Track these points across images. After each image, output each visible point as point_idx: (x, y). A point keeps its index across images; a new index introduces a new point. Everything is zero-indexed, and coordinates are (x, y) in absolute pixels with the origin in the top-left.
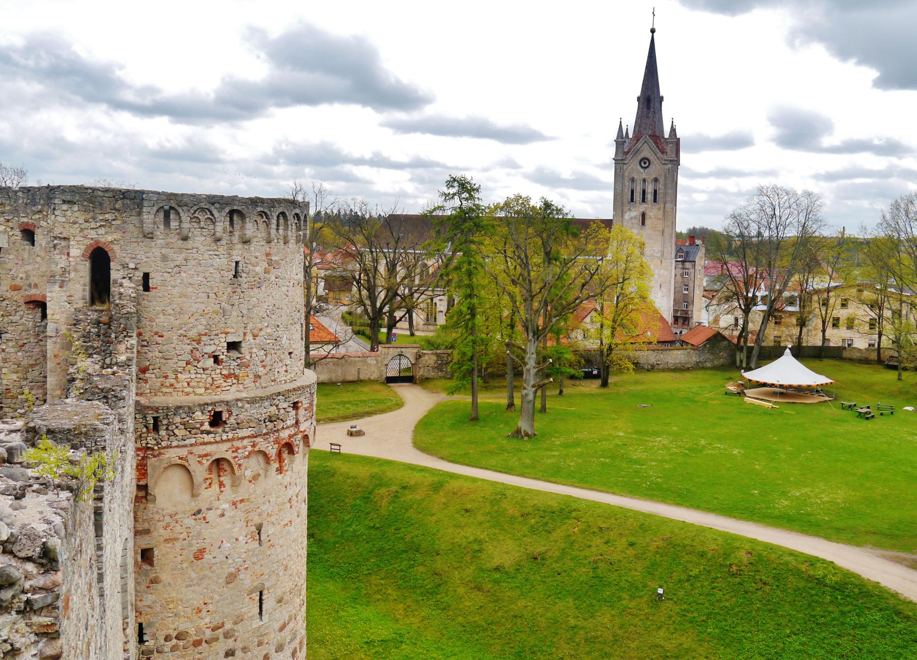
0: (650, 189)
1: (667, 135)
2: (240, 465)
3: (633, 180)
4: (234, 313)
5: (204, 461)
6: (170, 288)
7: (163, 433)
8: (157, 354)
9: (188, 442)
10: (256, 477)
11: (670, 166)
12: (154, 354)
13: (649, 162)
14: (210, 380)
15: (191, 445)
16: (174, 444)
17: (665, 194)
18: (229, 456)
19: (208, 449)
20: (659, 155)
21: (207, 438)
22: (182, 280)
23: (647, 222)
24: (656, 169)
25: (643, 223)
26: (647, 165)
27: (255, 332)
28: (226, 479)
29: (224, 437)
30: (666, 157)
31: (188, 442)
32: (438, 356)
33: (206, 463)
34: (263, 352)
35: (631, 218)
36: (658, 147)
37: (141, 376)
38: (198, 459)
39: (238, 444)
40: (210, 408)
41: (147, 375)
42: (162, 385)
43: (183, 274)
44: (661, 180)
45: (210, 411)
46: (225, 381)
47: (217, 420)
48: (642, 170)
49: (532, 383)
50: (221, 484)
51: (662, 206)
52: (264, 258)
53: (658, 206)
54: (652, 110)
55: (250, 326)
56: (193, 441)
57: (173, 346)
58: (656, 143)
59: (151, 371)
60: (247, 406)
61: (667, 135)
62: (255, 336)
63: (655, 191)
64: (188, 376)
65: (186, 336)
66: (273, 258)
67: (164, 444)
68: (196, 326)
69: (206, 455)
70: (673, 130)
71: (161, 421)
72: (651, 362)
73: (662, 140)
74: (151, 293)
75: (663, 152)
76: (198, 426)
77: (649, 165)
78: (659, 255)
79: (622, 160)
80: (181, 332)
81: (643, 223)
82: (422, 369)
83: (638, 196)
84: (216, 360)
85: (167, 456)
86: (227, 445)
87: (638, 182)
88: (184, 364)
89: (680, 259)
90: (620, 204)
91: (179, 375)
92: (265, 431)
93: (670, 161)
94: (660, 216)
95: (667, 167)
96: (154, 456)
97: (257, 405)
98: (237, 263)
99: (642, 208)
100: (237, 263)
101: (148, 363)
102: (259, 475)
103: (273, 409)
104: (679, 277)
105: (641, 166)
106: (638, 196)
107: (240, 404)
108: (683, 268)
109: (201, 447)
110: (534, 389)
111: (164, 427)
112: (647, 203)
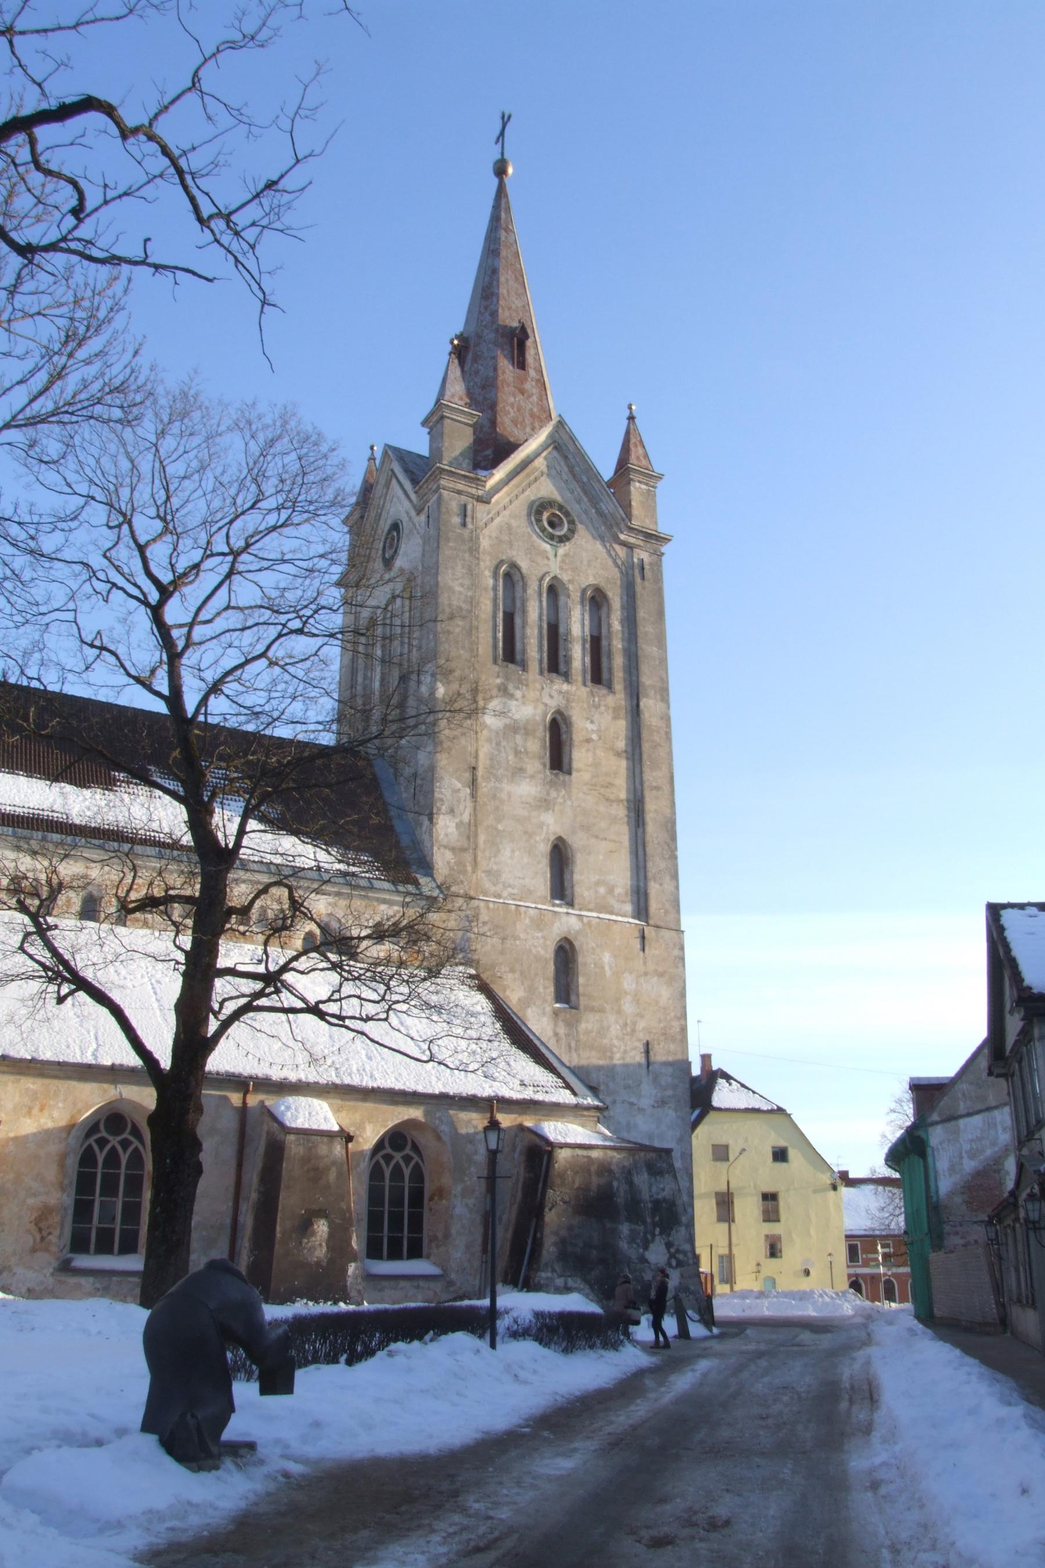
23: (580, 757)
54: (532, 373)
105: (543, 530)
112: (567, 677)
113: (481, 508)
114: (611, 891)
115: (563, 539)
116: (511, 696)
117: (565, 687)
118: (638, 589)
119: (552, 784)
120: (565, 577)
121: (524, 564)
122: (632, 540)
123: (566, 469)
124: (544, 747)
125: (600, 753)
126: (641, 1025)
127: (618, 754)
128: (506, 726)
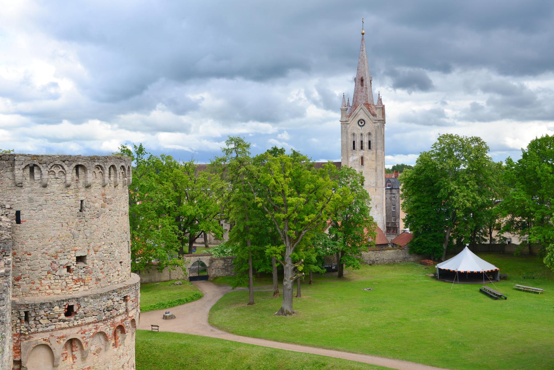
0: (366, 141)
1: (376, 103)
2: (87, 343)
3: (354, 134)
4: (81, 236)
5: (62, 341)
6: (35, 220)
7: (32, 322)
8: (27, 267)
9: (49, 328)
10: (98, 351)
11: (379, 124)
12: (24, 267)
13: (365, 122)
14: (64, 283)
15: (52, 330)
16: (40, 330)
17: (376, 143)
18: (79, 336)
19: (64, 332)
20: (371, 117)
21: (63, 325)
22: (44, 215)
23: (365, 163)
24: (369, 126)
25: (362, 164)
26: (363, 124)
27: (96, 248)
28: (77, 354)
29: (76, 324)
30: (376, 119)
31: (49, 328)
32: (225, 261)
33: (63, 342)
34: (101, 263)
35: (354, 161)
36: (370, 111)
37: (15, 283)
38: (57, 340)
39: (84, 328)
40: (65, 303)
41: (20, 282)
42: (31, 289)
43: (44, 211)
44: (373, 134)
45: (65, 306)
46: (75, 284)
47: (70, 311)
48: (360, 128)
49: (290, 277)
50: (74, 357)
51: (375, 152)
52: (101, 197)
53: (371, 152)
54: (365, 86)
55: (92, 245)
56: (53, 327)
57: (38, 261)
58: (368, 109)
59: (23, 279)
60: (91, 300)
61: (376, 103)
62: (96, 252)
63: (370, 142)
64: (49, 281)
65: (47, 254)
66: (107, 197)
67: (32, 330)
68: (54, 246)
69: (63, 337)
70: (380, 100)
71: (30, 314)
72: (372, 259)
73: (373, 107)
74: (22, 225)
75: (374, 115)
76: (57, 316)
77: (365, 124)
78: (374, 185)
79: (346, 121)
80: (44, 251)
81: (362, 164)
82: (214, 270)
83: (358, 146)
84: (69, 269)
85: (36, 338)
86: (77, 329)
87: (358, 136)
88: (46, 273)
89: (389, 188)
90: (346, 151)
91: (43, 281)
92: (104, 318)
93: (379, 120)
94: (374, 159)
95: (376, 125)
96: (26, 340)
97: (98, 300)
98: (82, 201)
99: (361, 153)
100: (82, 201)
101: (20, 274)
102: (101, 349)
103: (110, 302)
104: (389, 200)
105: (359, 125)
106: (358, 146)
107: (86, 300)
108: (391, 194)
109: (59, 331)
110: (292, 281)
111: (33, 319)
113: (348, 125)
114: (371, 183)
115: (363, 126)
116: (354, 156)
117: (363, 152)
118: (377, 131)
119: (361, 168)
120: (363, 133)
121: (356, 132)
122: (376, 122)
123: (363, 112)
124: (360, 162)
125: (369, 161)
126: (375, 202)
127: (372, 161)
128: (353, 161)
